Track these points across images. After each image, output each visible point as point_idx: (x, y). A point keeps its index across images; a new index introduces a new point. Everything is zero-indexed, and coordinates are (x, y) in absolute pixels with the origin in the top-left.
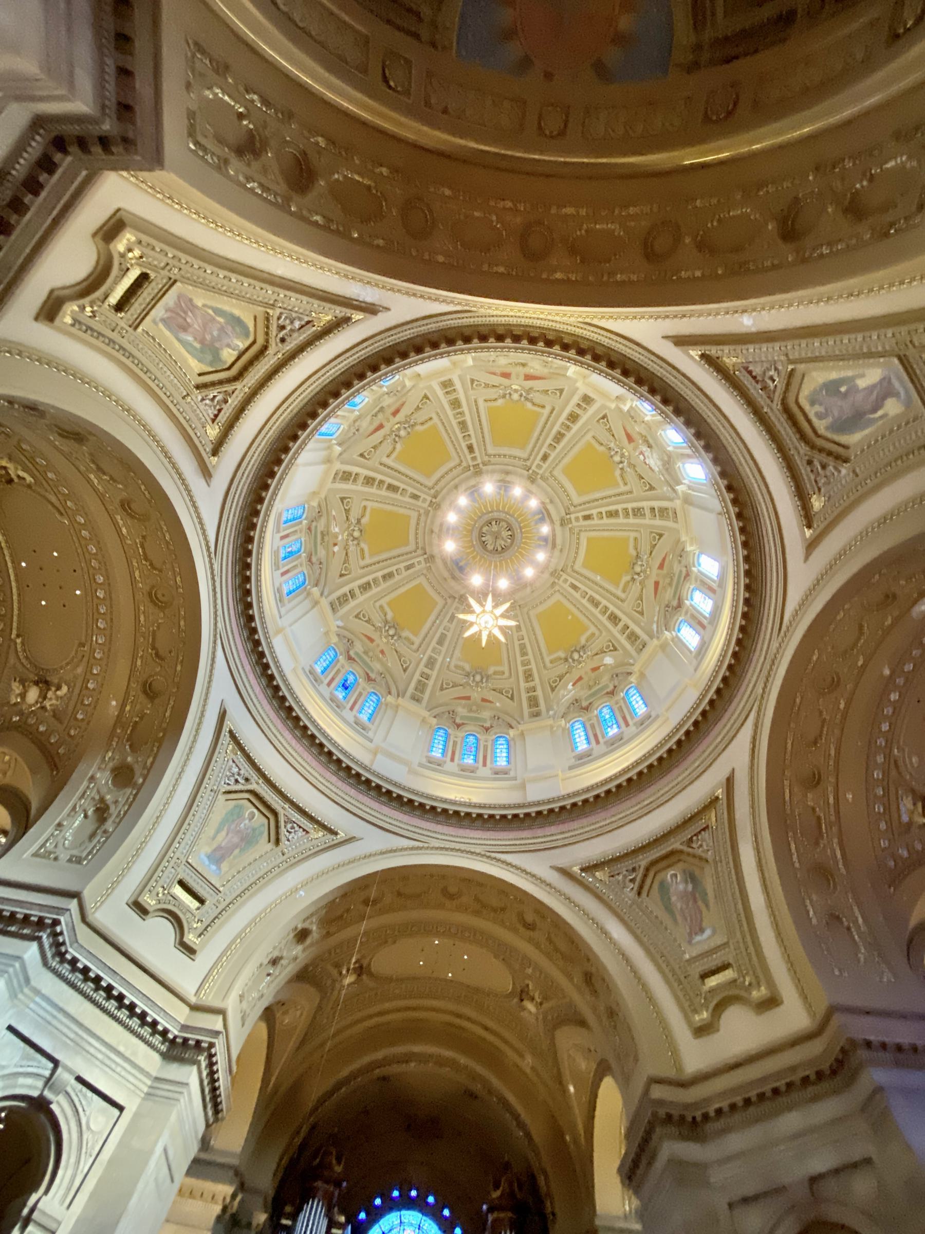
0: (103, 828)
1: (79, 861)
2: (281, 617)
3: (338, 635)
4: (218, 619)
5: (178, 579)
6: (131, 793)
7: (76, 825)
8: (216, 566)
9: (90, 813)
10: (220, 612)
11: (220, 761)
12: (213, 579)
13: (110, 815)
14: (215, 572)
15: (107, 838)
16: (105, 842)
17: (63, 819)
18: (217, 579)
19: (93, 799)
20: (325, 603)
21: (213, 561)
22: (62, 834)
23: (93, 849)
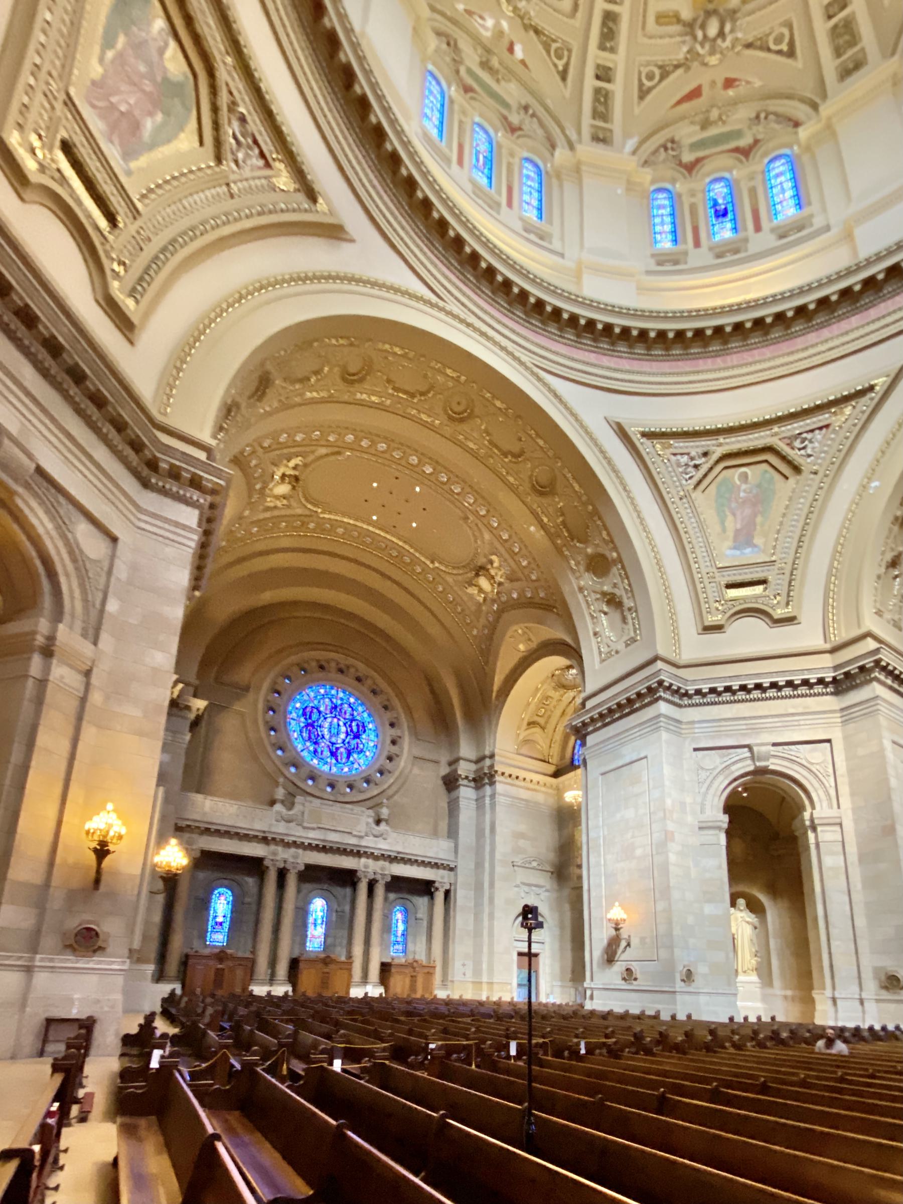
0: (625, 608)
1: (633, 640)
2: (562, 255)
3: (646, 163)
4: (517, 354)
5: (449, 371)
6: (618, 570)
7: (605, 624)
8: (456, 309)
9: (605, 609)
10: (510, 346)
11: (662, 469)
12: (469, 325)
13: (621, 596)
14: (462, 316)
15: (636, 611)
16: (637, 616)
17: (593, 629)
18: (471, 319)
19: (597, 599)
20: (587, 150)
21: (448, 308)
22: (603, 636)
23: (634, 625)
